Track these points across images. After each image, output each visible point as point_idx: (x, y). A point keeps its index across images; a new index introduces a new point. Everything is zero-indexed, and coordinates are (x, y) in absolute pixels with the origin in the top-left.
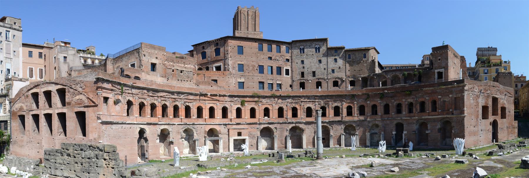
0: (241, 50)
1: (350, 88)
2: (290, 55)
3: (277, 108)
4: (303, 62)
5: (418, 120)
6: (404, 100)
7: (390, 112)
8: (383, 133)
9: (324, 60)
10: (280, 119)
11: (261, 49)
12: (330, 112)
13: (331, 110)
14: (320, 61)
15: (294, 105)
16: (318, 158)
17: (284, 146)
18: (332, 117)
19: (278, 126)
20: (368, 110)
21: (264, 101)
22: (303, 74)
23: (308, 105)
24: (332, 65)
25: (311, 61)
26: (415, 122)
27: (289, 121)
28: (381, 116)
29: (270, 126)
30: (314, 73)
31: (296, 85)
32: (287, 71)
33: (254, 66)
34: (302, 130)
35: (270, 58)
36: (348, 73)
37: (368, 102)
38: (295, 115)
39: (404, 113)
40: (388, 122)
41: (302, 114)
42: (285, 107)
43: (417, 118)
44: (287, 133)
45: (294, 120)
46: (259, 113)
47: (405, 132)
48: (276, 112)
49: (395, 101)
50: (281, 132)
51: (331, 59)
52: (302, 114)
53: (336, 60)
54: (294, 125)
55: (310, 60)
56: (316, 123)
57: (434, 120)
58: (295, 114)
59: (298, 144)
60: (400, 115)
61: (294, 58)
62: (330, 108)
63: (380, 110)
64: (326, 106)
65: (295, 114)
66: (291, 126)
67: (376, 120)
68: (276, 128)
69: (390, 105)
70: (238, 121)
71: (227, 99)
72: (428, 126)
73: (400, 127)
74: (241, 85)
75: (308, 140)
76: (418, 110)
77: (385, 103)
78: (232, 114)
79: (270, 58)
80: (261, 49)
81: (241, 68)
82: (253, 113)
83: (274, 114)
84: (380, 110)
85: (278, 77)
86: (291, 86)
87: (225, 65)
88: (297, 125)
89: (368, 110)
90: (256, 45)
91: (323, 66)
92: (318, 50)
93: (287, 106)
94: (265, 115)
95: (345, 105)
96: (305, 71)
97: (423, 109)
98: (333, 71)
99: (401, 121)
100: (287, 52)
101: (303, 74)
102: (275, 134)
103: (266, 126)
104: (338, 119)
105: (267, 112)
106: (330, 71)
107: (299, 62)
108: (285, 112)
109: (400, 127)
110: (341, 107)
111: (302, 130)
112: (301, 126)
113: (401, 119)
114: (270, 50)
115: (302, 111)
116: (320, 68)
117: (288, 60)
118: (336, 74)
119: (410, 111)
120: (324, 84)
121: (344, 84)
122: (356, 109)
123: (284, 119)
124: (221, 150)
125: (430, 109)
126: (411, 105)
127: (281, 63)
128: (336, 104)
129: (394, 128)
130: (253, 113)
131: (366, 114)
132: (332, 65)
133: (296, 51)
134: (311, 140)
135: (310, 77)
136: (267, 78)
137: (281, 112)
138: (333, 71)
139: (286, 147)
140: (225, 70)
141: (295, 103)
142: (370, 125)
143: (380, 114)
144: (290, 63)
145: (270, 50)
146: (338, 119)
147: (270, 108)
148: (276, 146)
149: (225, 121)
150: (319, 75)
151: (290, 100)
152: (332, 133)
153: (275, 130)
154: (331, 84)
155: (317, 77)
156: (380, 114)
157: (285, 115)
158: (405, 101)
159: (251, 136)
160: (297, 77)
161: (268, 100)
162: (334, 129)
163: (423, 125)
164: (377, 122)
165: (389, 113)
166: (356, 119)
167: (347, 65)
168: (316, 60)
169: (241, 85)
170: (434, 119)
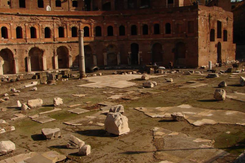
1: (72, 9)
3: (15, 27)
8: (119, 53)
10: (19, 39)
12: (68, 33)
13: (68, 29)
15: (32, 25)
17: (25, 69)
18: (70, 38)
20: (104, 32)
23: (46, 26)
27: (29, 41)
29: (9, 47)
34: (42, 52)
37: (105, 24)
38: (33, 35)
41: (40, 34)
42: (23, 27)
43: (152, 39)
44: (26, 55)
45: (33, 41)
47: (140, 52)
54: (33, 46)
56: (79, 42)
58: (33, 35)
62: (68, 29)
63: (116, 32)
64: (65, 27)
68: (15, 50)
69: (126, 26)
72: (163, 46)
75: (48, 61)
83: (12, 34)
84: (116, 32)
88: (37, 46)
89: (104, 32)
94: (2, 37)
95: (82, 26)
102: (15, 56)
103: (4, 47)
108: (24, 33)
109: (135, 47)
110: (78, 27)
111: (42, 52)
112: (41, 47)
115: (41, 31)
122: (93, 30)
123: (23, 39)
125: (165, 32)
128: (74, 25)
131: (102, 35)
134: (51, 61)
139: (27, 70)
141: (33, 22)
142: (107, 45)
147: (8, 28)
148: (17, 69)
151: (27, 19)
152: (70, 53)
153: (14, 52)
156: (116, 35)
157: (23, 35)
158: (140, 24)
162: (72, 49)
163: (157, 46)
164: (113, 43)
166: (92, 39)
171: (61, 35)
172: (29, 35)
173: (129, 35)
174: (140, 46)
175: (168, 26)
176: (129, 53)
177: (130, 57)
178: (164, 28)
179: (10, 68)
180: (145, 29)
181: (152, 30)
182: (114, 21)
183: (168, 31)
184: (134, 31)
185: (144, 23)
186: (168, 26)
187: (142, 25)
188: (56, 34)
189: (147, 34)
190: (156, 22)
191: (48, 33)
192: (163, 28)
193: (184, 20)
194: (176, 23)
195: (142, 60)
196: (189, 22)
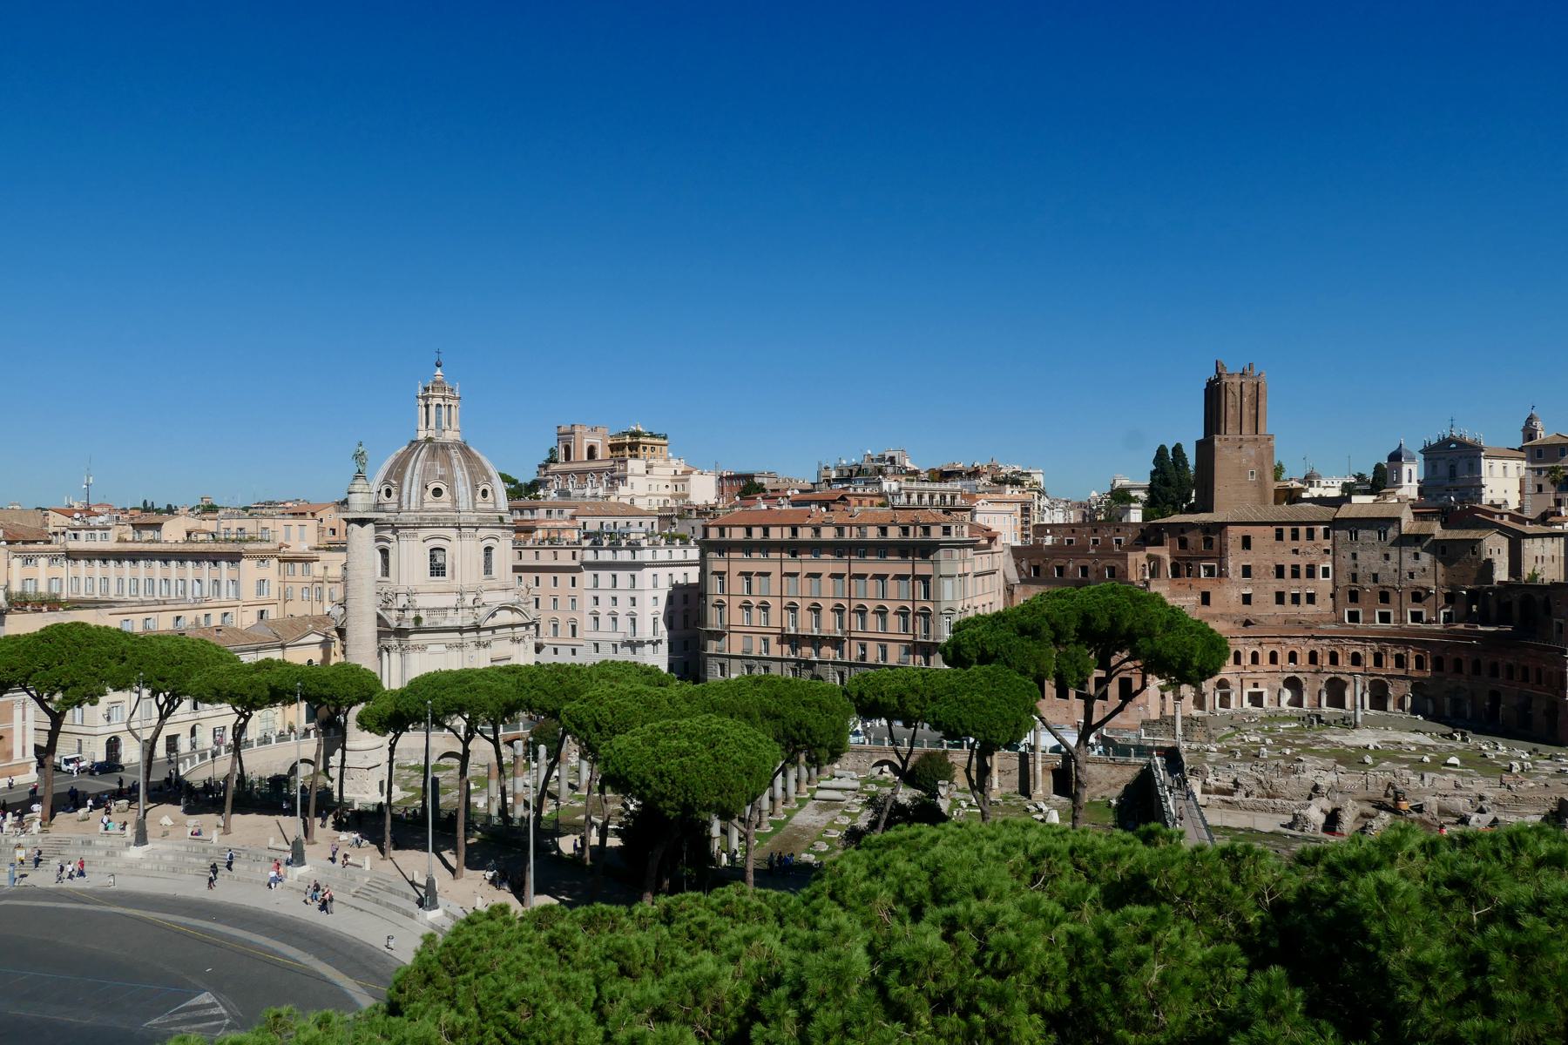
0: (1246, 542)
2: (1330, 541)
4: (1354, 556)
9: (1394, 553)
11: (1279, 536)
14: (1387, 557)
16: (1355, 727)
19: (1308, 676)
21: (1288, 641)
22: (1354, 577)
24: (1409, 564)
25: (1371, 557)
30: (1375, 577)
31: (1343, 597)
32: (1326, 571)
33: (1267, 568)
34: (1345, 684)
35: (1296, 551)
36: (1441, 580)
41: (1344, 663)
44: (1322, 686)
45: (1332, 669)
46: (1283, 658)
48: (1306, 658)
50: (1313, 686)
51: (1407, 554)
52: (1344, 663)
53: (1417, 556)
55: (1369, 553)
58: (1334, 659)
59: (1337, 700)
61: (1338, 547)
63: (1467, 668)
65: (1334, 659)
66: (1327, 677)
70: (1254, 668)
71: (1241, 641)
73: (1495, 697)
74: (1247, 599)
78: (1246, 660)
79: (1296, 551)
80: (1279, 536)
81: (1247, 571)
82: (1273, 658)
83: (1303, 659)
84: (1467, 668)
85: (1310, 582)
86: (1332, 596)
87: (1220, 567)
90: (1272, 530)
91: (1392, 564)
92: (1383, 534)
93: (1323, 648)
96: (1360, 571)
97: (1526, 679)
98: (1411, 575)
100: (1326, 536)
101: (1354, 577)
104: (1401, 672)
105: (1293, 657)
106: (1405, 574)
107: (1349, 555)
109: (1495, 697)
111: (1345, 684)
112: (1343, 677)
114: (1295, 536)
116: (1386, 568)
117: (1327, 551)
118: (1417, 581)
120: (1394, 597)
121: (1432, 599)
124: (1233, 705)
126: (1510, 669)
127: (1314, 558)
130: (1273, 658)
132: (1409, 564)
133: (1342, 534)
135: (1369, 585)
136: (1290, 586)
137: (1313, 657)
138: (1411, 575)
140: (1221, 575)
144: (1330, 557)
145: (1295, 536)
146: (1401, 672)
148: (1305, 702)
149: (1238, 668)
150: (1387, 580)
151: (1326, 642)
154: (1407, 598)
155: (1380, 583)
159: (1271, 688)
160: (1344, 581)
161: (1295, 641)
167: (1440, 565)
168: (1378, 554)
169: (1247, 599)
171: (1378, 661)
172: (1327, 660)
175: (1539, 672)
179: (1297, 702)
180: (1510, 670)
183: (1539, 682)
184: (1494, 672)
186: (1539, 672)
188: (1370, 662)
191: (1356, 659)
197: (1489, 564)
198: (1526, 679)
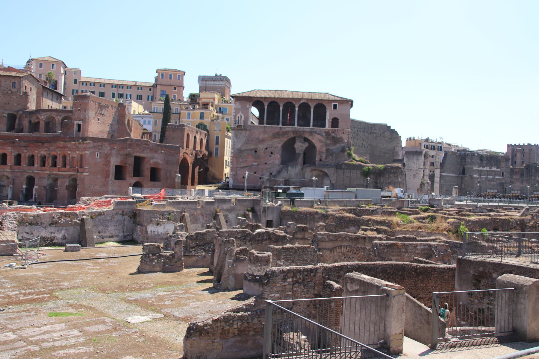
5: (49, 175)
6: (37, 152)
7: (22, 163)
26: (46, 176)
28: (11, 167)
39: (36, 166)
40: (19, 174)
43: (48, 172)
49: (28, 151)
57: (64, 177)
60: (32, 168)
67: (4, 171)
69: (22, 155)
72: (59, 181)
73: (31, 181)
76: (50, 165)
77: (17, 153)
99: (32, 175)
109: (31, 181)
113: (33, 172)
119: (43, 164)
129: (25, 182)
143: (9, 164)
156: (9, 164)
164: (5, 173)
165: (20, 165)
170: (63, 175)
173: (24, 165)
174: (36, 180)
175: (64, 158)
176: (24, 187)
177: (24, 192)
178: (61, 160)
181: (49, 162)
182: (9, 148)
183: (65, 165)
185: (42, 152)
186: (64, 158)
187: (39, 155)
189: (44, 165)
190: (54, 153)
192: (60, 161)
193: (77, 152)
194: (71, 156)
195: (36, 197)
196: (82, 155)
197: (26, 94)
198: (55, 165)
